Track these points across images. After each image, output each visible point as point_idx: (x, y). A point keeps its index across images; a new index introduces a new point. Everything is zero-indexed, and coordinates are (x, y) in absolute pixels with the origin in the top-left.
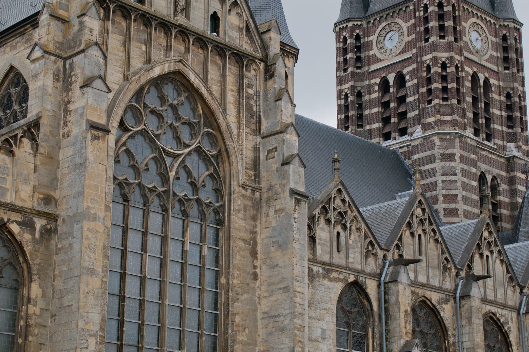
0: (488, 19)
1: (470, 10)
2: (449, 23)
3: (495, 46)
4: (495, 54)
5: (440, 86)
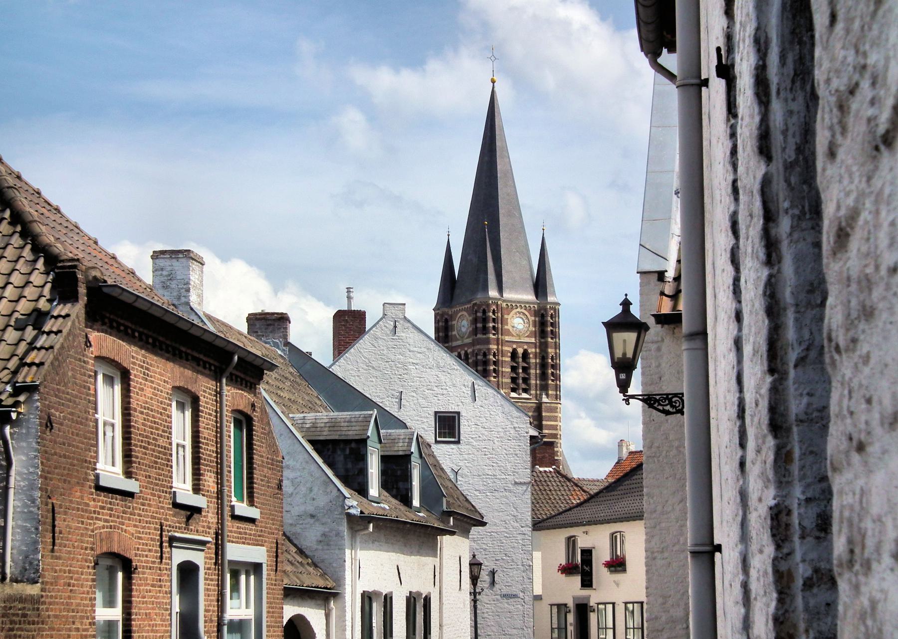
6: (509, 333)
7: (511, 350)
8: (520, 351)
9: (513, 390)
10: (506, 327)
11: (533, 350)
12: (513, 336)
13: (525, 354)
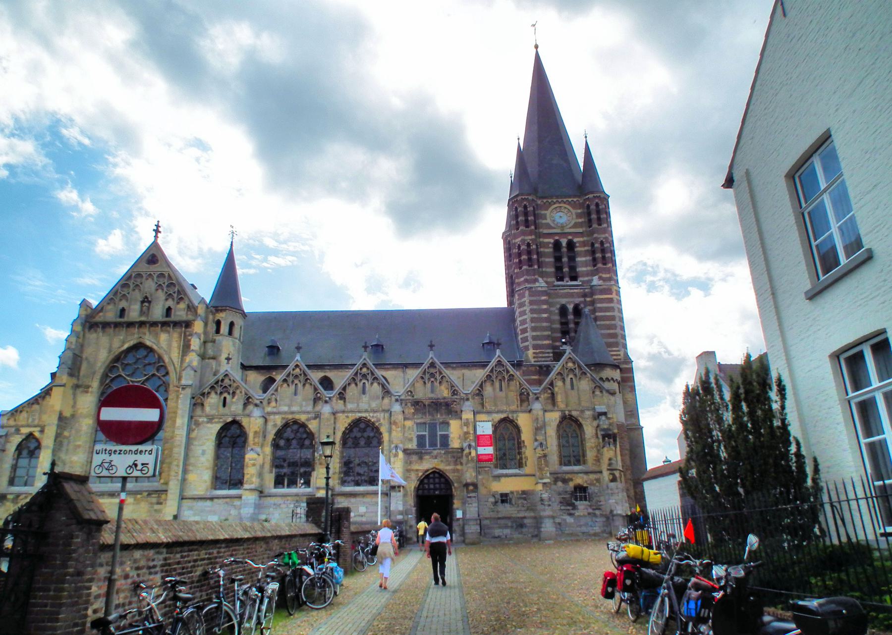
0: (570, 200)
1: (550, 201)
2: (531, 218)
3: (579, 216)
4: (580, 220)
5: (517, 260)
6: (548, 226)
7: (552, 241)
8: (564, 242)
9: (561, 279)
10: (544, 221)
11: (581, 239)
12: (554, 228)
13: (571, 245)
